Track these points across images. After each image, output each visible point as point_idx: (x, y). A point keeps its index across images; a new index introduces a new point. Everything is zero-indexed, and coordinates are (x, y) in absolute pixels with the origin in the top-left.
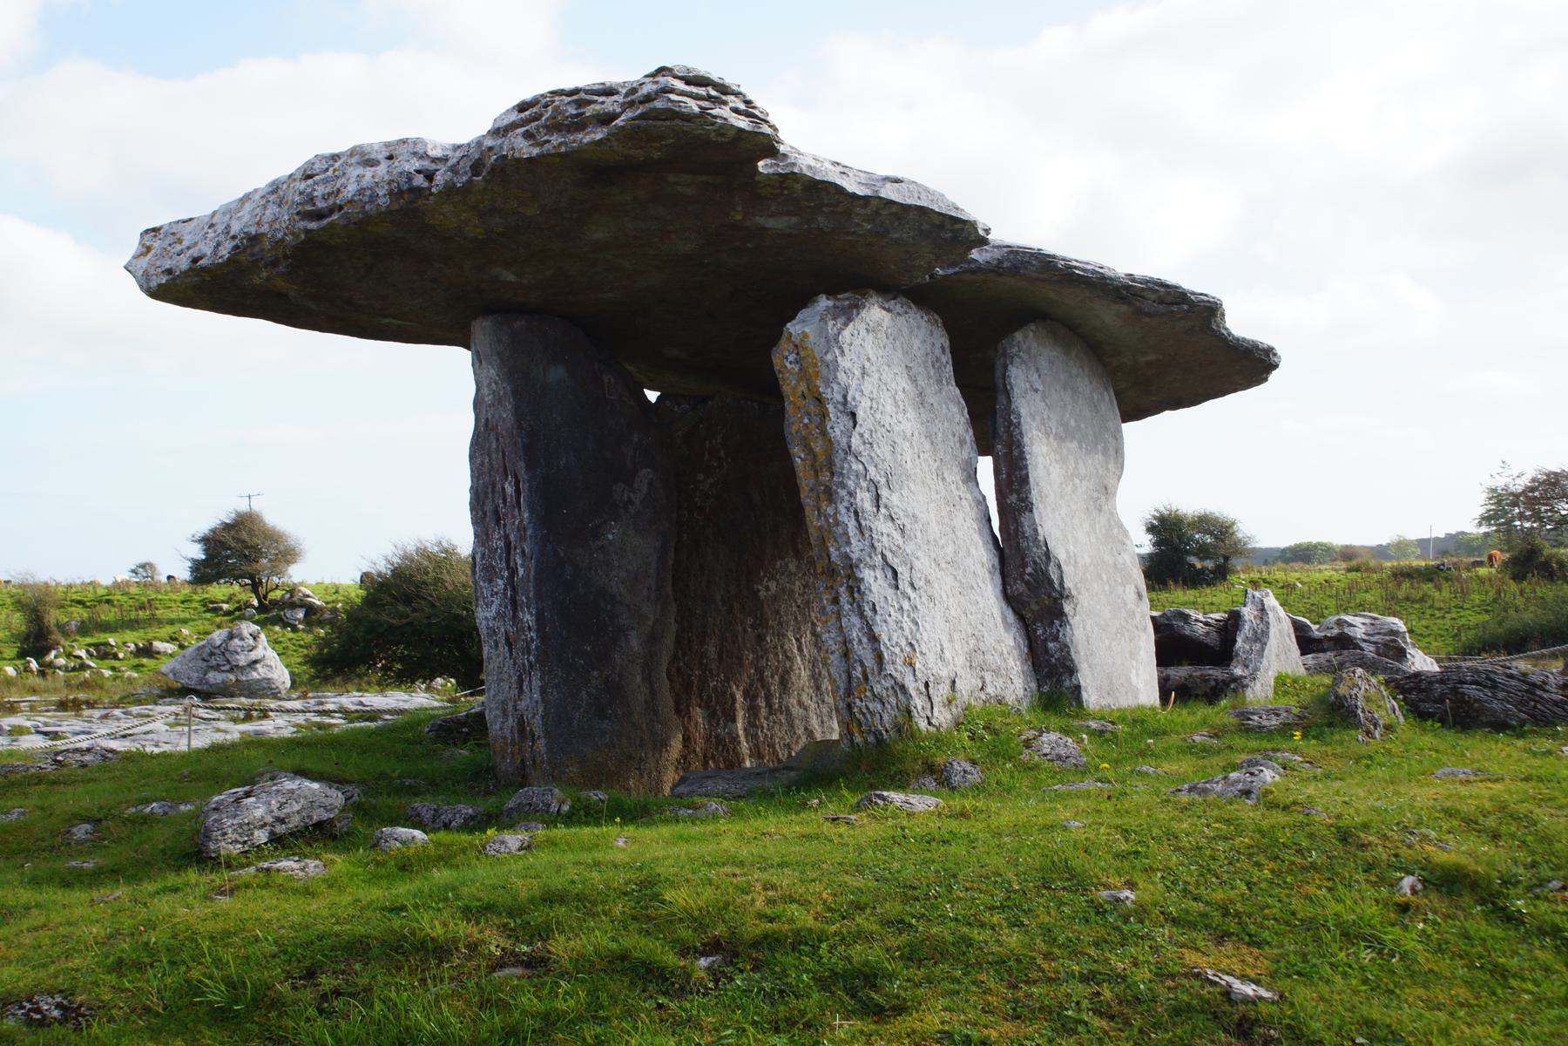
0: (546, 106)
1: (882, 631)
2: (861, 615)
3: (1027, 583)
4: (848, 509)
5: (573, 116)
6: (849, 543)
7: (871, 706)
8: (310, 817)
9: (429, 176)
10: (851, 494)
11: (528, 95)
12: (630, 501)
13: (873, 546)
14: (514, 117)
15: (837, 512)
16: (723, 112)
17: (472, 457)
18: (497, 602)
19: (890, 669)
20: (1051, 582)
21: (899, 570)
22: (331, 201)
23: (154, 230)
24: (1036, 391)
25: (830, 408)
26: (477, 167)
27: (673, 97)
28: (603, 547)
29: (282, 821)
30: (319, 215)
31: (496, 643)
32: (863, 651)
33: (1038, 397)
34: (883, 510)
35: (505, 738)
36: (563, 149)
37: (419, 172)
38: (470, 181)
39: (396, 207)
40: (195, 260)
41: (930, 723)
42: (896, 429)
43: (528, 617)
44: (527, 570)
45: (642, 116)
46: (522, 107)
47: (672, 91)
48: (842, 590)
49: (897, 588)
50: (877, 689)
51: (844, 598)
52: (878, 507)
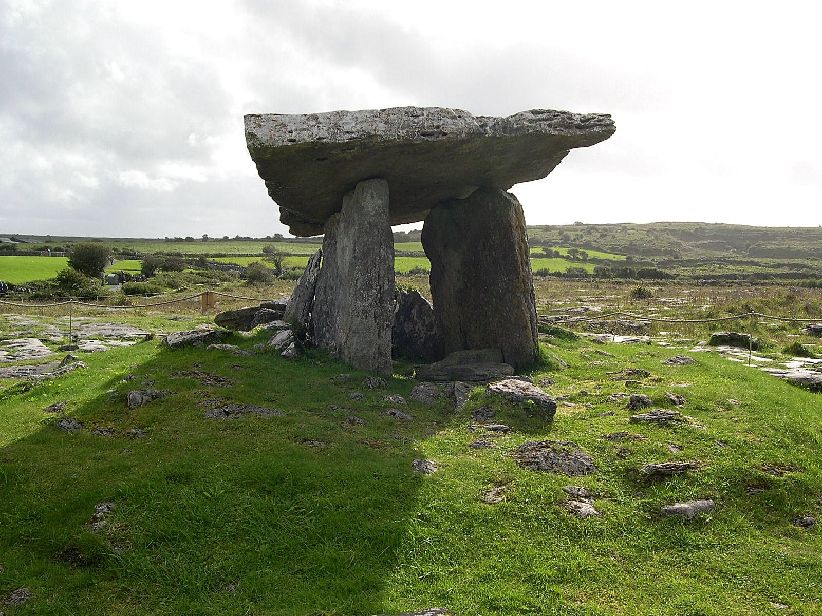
11: (537, 108)
14: (532, 116)
31: (366, 316)
40: (320, 139)
46: (535, 112)
48: (529, 298)
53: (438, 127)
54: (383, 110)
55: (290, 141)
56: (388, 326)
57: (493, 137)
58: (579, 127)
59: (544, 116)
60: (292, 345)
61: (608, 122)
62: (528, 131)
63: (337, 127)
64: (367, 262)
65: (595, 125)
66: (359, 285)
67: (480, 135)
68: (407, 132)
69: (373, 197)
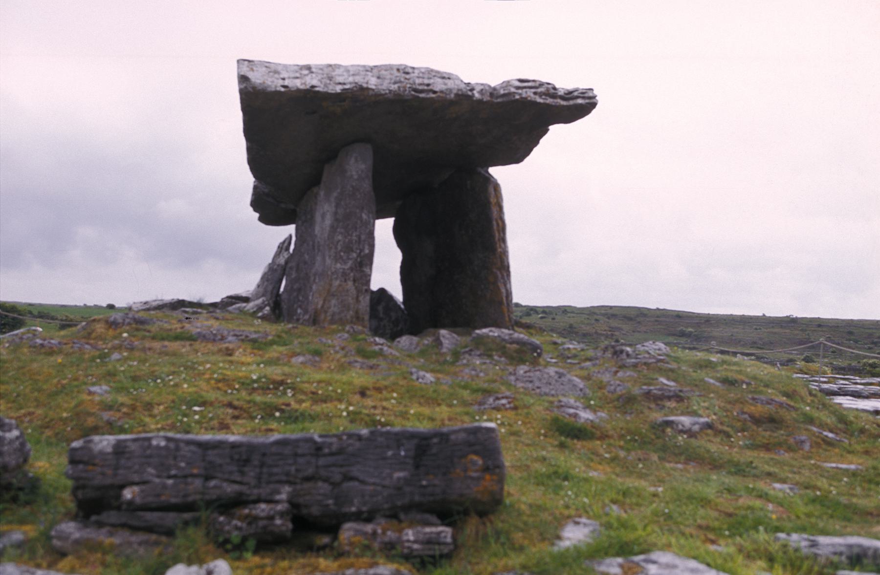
30: (416, 90)
40: (313, 87)
53: (428, 85)
54: (375, 66)
55: (284, 86)
57: (480, 102)
58: (562, 98)
59: (530, 84)
60: (268, 308)
61: (591, 95)
63: (330, 78)
65: (577, 97)
66: (339, 248)
67: (468, 96)
68: (399, 87)
69: (356, 161)
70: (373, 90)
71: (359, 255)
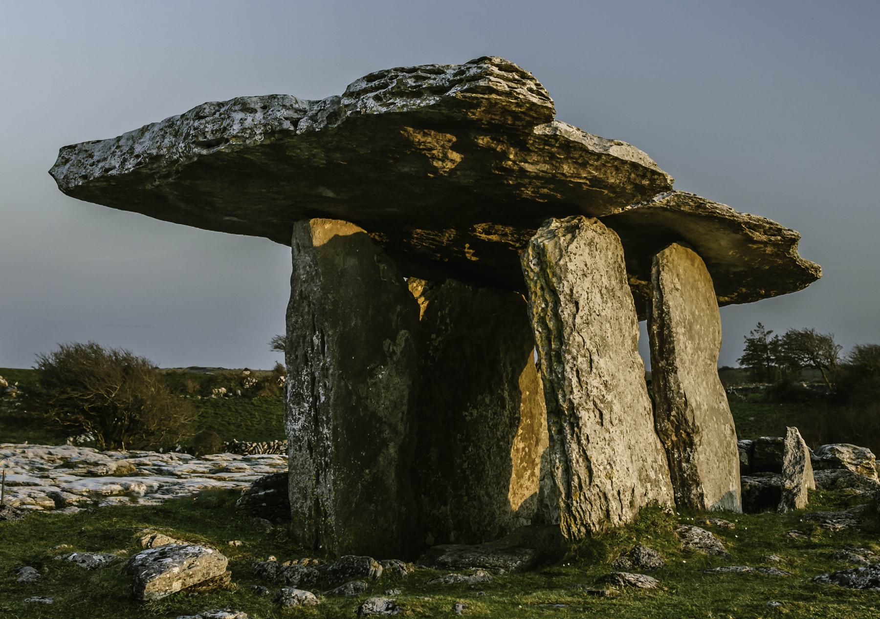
0: (391, 79)
1: (593, 454)
2: (579, 443)
3: (672, 422)
4: (572, 369)
5: (412, 87)
6: (572, 392)
7: (583, 506)
8: (208, 574)
9: (295, 123)
10: (574, 358)
11: (375, 70)
12: (394, 352)
13: (588, 395)
14: (364, 85)
15: (564, 370)
16: (522, 91)
17: (288, 317)
18: (303, 419)
19: (597, 481)
20: (686, 422)
21: (604, 412)
22: (218, 135)
23: (70, 147)
24: (677, 290)
25: (562, 297)
26: (333, 116)
27: (492, 78)
28: (375, 384)
29: (191, 576)
31: (300, 447)
32: (580, 469)
33: (678, 294)
34: (594, 370)
35: (304, 514)
36: (405, 109)
37: (286, 119)
38: (326, 127)
39: (268, 142)
40: (107, 170)
41: (620, 519)
42: (603, 314)
43: (326, 431)
44: (328, 397)
45: (469, 90)
46: (370, 78)
47: (491, 74)
49: (602, 425)
50: (588, 494)
51: (568, 430)
52: (591, 367)
53: (225, 129)
55: (85, 177)
56: (326, 463)
62: (345, 112)
63: (131, 150)
64: (297, 357)
70: (163, 156)
71: (313, 405)
